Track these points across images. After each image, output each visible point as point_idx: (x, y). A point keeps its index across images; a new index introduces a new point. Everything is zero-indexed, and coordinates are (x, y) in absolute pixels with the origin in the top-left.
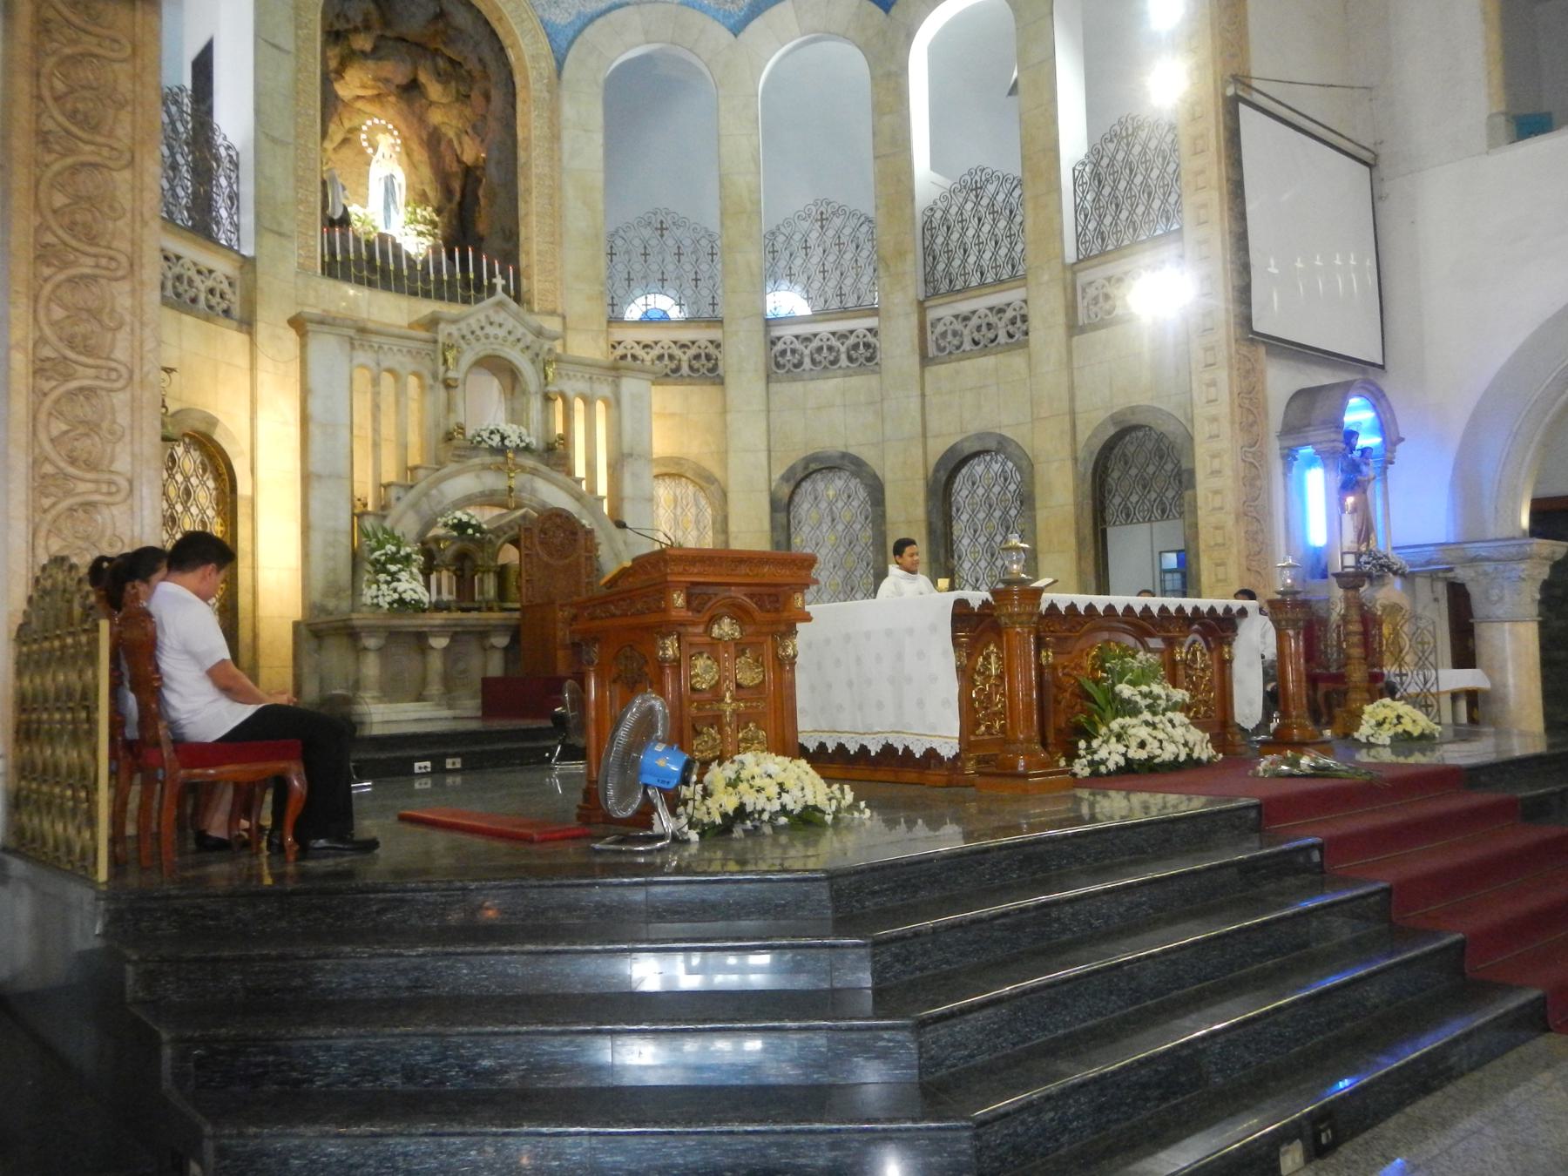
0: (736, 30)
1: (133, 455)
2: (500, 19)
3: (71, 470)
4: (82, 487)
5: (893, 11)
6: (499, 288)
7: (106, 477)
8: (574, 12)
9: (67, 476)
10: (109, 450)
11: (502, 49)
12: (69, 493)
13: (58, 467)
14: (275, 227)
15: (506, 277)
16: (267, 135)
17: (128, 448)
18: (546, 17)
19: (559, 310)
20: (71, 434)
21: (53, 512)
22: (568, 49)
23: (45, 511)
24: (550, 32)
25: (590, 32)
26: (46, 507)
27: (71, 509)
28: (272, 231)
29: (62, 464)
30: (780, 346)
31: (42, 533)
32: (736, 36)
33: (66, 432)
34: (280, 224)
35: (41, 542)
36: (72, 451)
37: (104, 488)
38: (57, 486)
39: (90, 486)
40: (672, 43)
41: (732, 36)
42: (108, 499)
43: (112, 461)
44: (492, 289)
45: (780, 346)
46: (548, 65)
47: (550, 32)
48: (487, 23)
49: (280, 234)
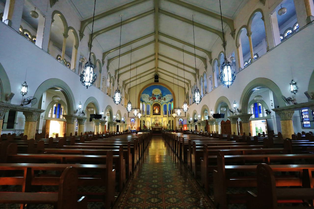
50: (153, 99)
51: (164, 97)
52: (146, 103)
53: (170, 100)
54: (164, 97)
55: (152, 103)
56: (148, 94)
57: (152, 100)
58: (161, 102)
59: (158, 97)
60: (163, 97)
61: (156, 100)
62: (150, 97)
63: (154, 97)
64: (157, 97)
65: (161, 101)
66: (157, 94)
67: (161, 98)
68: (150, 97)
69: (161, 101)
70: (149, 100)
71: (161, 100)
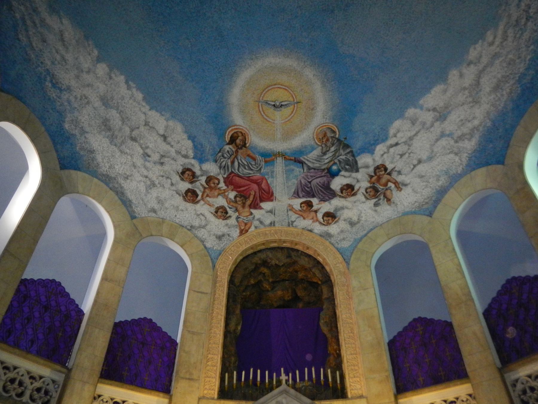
0: (430, 215)
2: (319, 255)
5: (506, 163)
6: (284, 382)
8: (352, 240)
11: (323, 267)
14: (188, 376)
15: (287, 374)
16: (189, 331)
18: (339, 246)
19: (364, 394)
22: (351, 257)
24: (341, 251)
25: (360, 246)
28: (186, 379)
30: (519, 386)
32: (431, 217)
34: (191, 374)
40: (401, 234)
41: (429, 218)
44: (279, 383)
45: (519, 386)
46: (342, 266)
47: (341, 251)
48: (315, 259)
49: (189, 379)
50: (243, 195)
51: (364, 160)
52: (141, 211)
53: (469, 145)
54: (364, 160)
55: (219, 238)
56: (175, 115)
57: (221, 201)
58: (333, 229)
59: (298, 170)
60: (354, 167)
61: (266, 205)
62: (201, 161)
63: (249, 179)
64: (288, 172)
65: (331, 216)
66: (287, 136)
67: (337, 184)
68: (201, 161)
69: (331, 216)
70: (179, 200)
71: (336, 202)
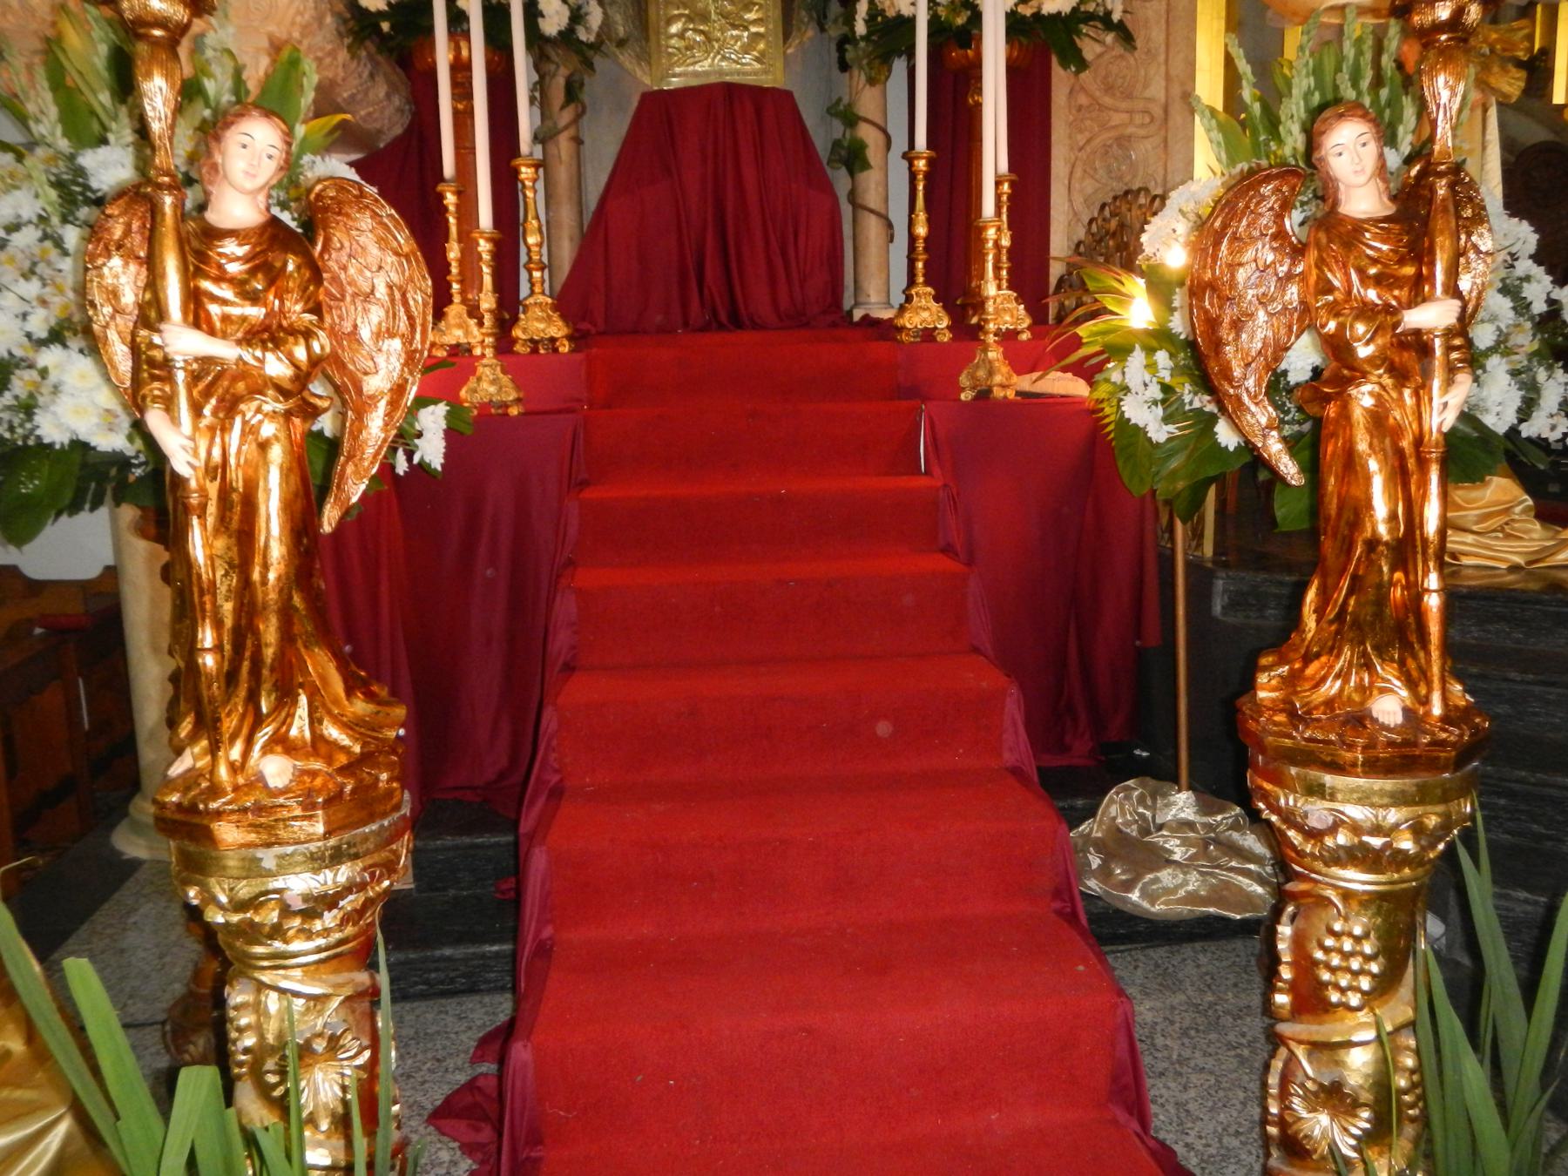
1: (1168, 78)
3: (1107, 100)
4: (1117, 119)
7: (1140, 105)
9: (1102, 108)
10: (1142, 73)
12: (1104, 127)
13: (1092, 97)
17: (1163, 68)
20: (1107, 57)
21: (1088, 149)
23: (1080, 149)
26: (1081, 144)
27: (1106, 149)
29: (1098, 94)
31: (1078, 173)
33: (1100, 56)
35: (1076, 185)
36: (1106, 77)
37: (1138, 119)
38: (1092, 119)
39: (1125, 117)
42: (1142, 132)
43: (1146, 86)
